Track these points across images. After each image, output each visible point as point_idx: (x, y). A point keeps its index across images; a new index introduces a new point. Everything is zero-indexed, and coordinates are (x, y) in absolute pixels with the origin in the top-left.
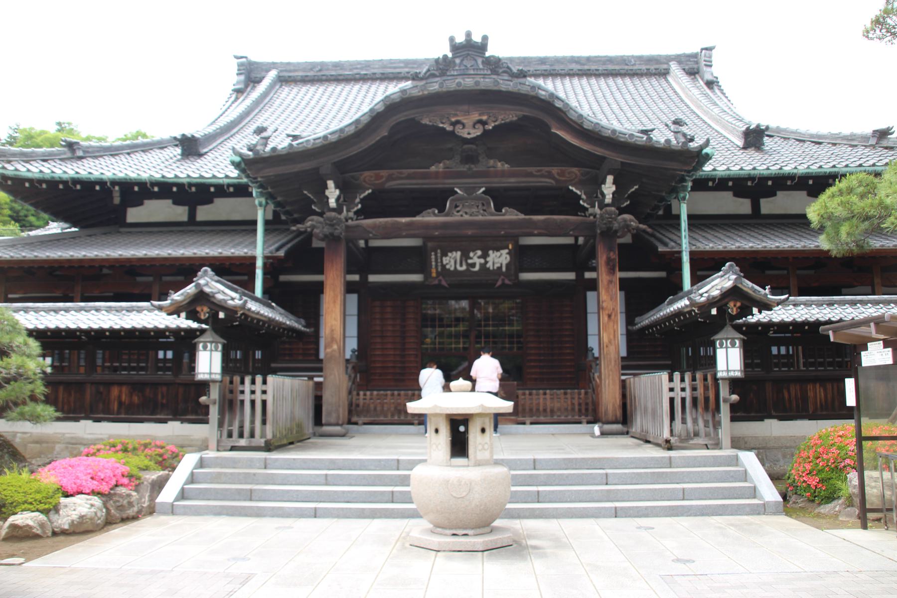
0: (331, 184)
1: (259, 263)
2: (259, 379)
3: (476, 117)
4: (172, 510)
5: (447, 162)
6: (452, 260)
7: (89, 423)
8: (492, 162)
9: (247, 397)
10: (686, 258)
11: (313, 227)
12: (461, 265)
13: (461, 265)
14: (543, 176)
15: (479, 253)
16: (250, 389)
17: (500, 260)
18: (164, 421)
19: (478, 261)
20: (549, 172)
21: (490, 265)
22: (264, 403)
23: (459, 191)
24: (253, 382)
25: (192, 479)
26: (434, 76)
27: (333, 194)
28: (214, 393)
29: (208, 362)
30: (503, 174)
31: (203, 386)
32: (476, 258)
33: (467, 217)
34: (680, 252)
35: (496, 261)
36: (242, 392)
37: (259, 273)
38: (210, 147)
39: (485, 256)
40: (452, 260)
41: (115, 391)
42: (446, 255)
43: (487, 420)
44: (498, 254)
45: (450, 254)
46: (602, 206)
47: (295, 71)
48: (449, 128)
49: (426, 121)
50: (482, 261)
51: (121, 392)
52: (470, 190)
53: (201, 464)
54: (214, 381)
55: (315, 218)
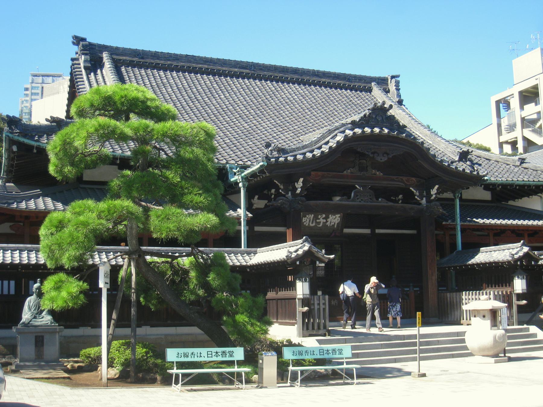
5: (352, 169)
10: (459, 228)
12: (312, 223)
13: (312, 223)
15: (324, 216)
17: (334, 221)
19: (322, 221)
20: (402, 179)
21: (328, 224)
23: (358, 187)
32: (321, 220)
33: (363, 203)
34: (457, 225)
39: (326, 218)
42: (305, 217)
44: (334, 217)
45: (307, 216)
46: (429, 201)
50: (325, 221)
55: (282, 198)
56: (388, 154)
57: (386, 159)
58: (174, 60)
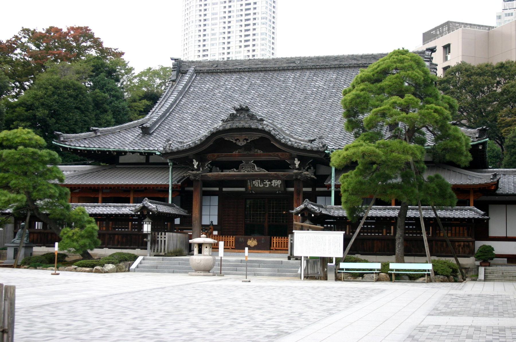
0: (194, 160)
1: (170, 188)
2: (163, 233)
3: (244, 137)
4: (134, 271)
7: (107, 249)
8: (256, 150)
9: (160, 239)
12: (261, 185)
13: (261, 185)
14: (275, 156)
18: (135, 249)
21: (273, 185)
25: (141, 263)
26: (229, 121)
27: (196, 164)
28: (149, 238)
29: (147, 228)
30: (260, 155)
31: (146, 235)
33: (246, 173)
37: (170, 191)
38: (155, 128)
39: (270, 181)
40: (257, 183)
41: (116, 237)
47: (203, 66)
48: (234, 142)
49: (226, 139)
50: (270, 183)
51: (118, 237)
52: (247, 162)
53: (144, 259)
54: (149, 234)
56: (247, 140)
57: (245, 143)
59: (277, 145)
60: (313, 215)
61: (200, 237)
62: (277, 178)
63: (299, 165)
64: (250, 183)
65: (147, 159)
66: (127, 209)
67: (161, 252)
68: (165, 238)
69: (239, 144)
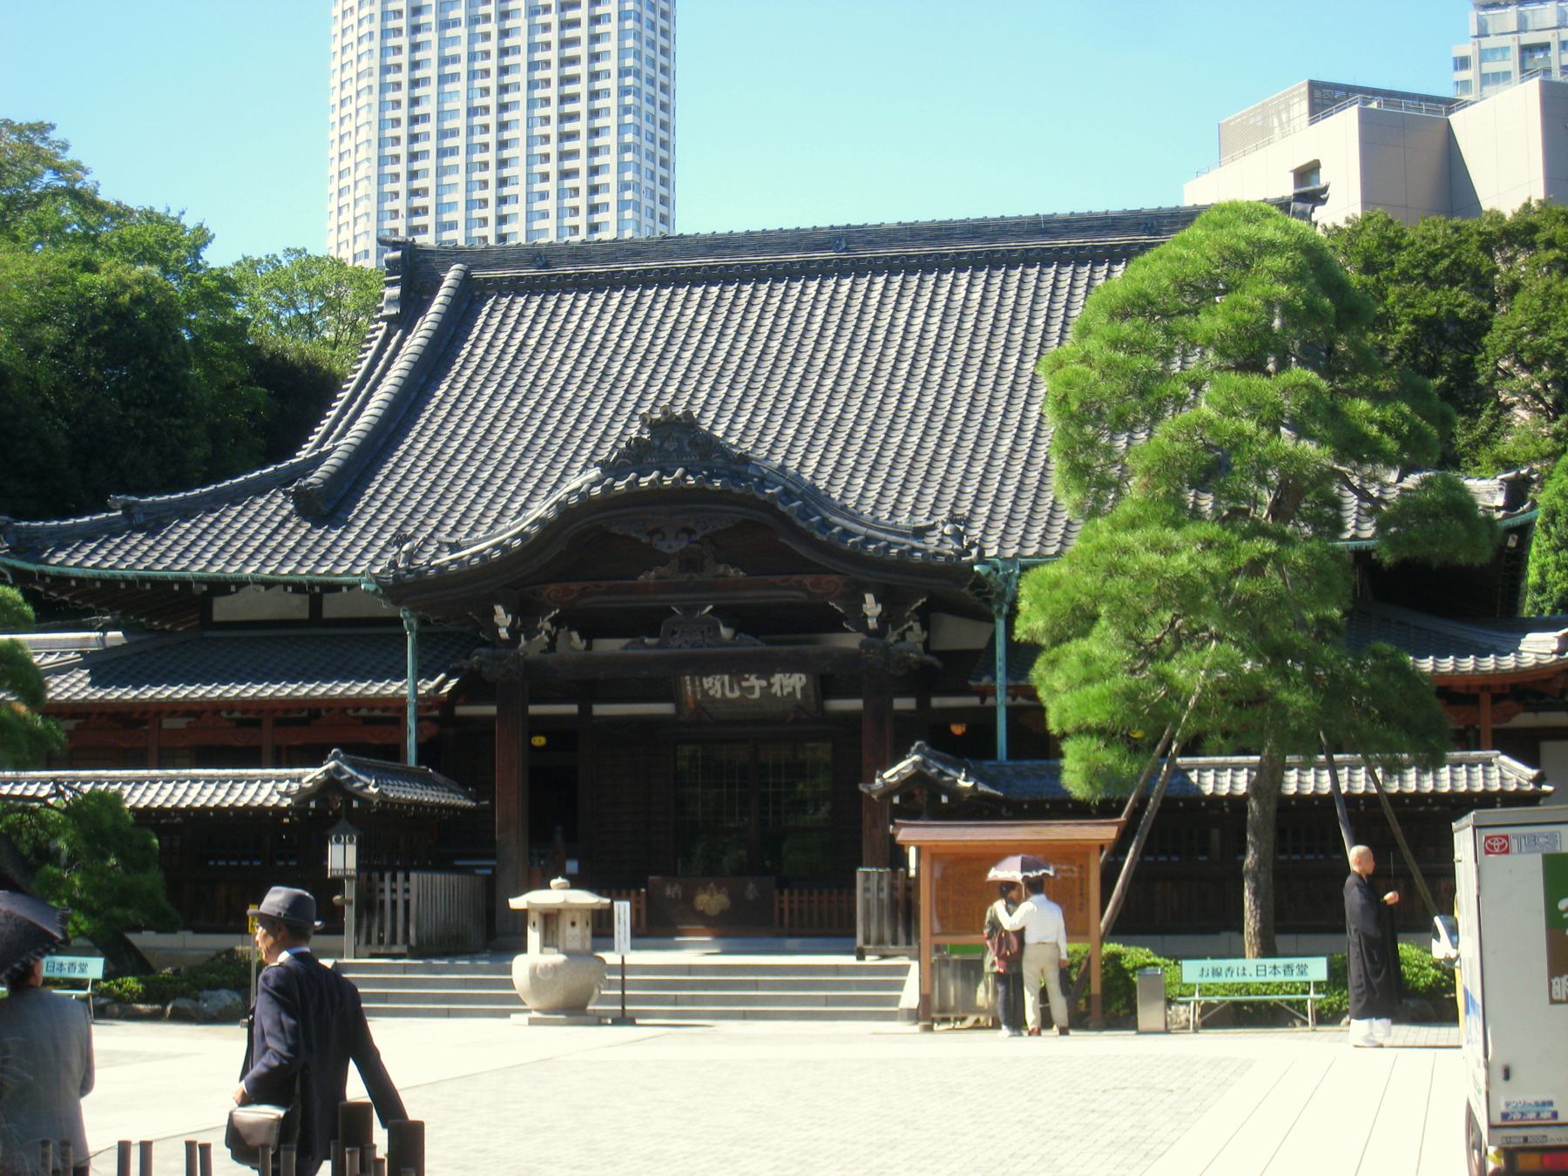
0: (499, 609)
1: (410, 711)
5: (662, 570)
6: (716, 686)
8: (721, 569)
9: (387, 896)
11: (481, 663)
12: (732, 690)
16: (390, 889)
21: (776, 689)
22: (407, 903)
24: (394, 879)
27: (502, 618)
33: (687, 650)
35: (785, 682)
36: (382, 891)
37: (411, 724)
43: (578, 915)
48: (645, 540)
49: (615, 529)
50: (764, 683)
52: (690, 610)
54: (350, 878)
55: (483, 650)
56: (689, 532)
58: (625, 258)
59: (801, 550)
60: (944, 799)
61: (548, 887)
62: (790, 667)
63: (880, 618)
64: (693, 683)
65: (316, 604)
66: (265, 788)
67: (393, 941)
68: (407, 891)
69: (663, 547)
